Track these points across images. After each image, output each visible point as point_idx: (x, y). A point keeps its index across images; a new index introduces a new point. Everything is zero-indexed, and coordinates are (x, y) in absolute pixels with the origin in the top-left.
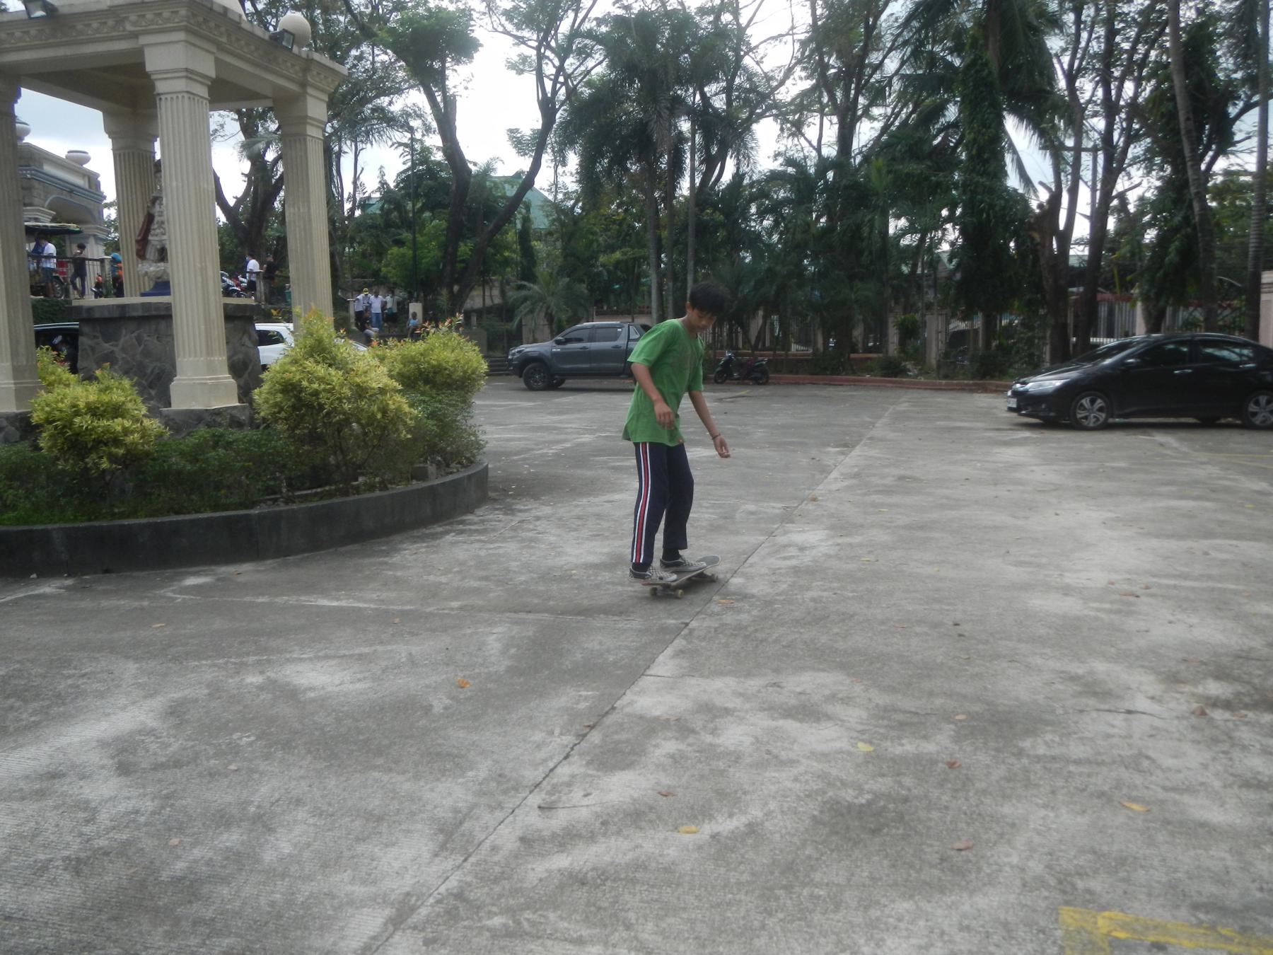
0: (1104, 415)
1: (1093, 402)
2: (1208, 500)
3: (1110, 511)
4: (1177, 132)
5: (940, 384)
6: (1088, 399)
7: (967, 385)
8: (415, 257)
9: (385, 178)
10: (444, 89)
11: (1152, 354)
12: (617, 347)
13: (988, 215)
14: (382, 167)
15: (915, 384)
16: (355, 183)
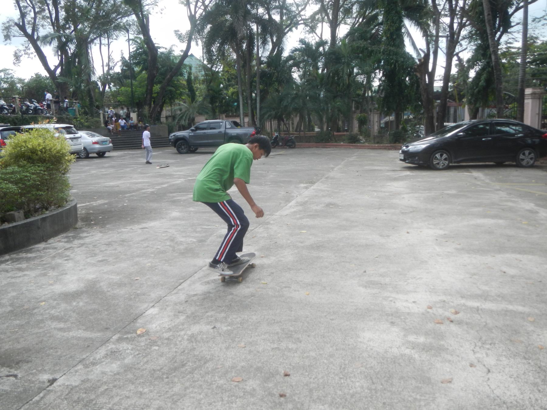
0: (447, 162)
1: (441, 155)
2: (501, 218)
3: (441, 229)
4: (483, 21)
5: (375, 146)
6: (439, 154)
7: (388, 146)
8: (132, 91)
9: (124, 55)
10: (142, 12)
11: (472, 130)
12: (220, 132)
13: (395, 66)
14: (122, 51)
15: (364, 146)
16: (109, 58)
